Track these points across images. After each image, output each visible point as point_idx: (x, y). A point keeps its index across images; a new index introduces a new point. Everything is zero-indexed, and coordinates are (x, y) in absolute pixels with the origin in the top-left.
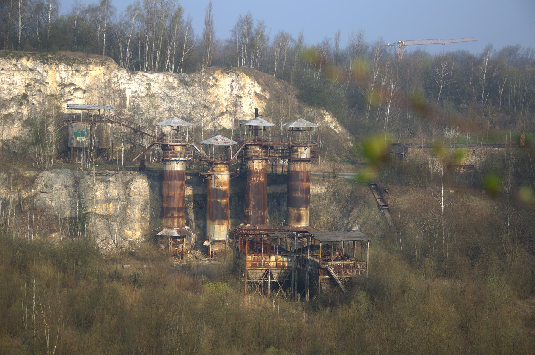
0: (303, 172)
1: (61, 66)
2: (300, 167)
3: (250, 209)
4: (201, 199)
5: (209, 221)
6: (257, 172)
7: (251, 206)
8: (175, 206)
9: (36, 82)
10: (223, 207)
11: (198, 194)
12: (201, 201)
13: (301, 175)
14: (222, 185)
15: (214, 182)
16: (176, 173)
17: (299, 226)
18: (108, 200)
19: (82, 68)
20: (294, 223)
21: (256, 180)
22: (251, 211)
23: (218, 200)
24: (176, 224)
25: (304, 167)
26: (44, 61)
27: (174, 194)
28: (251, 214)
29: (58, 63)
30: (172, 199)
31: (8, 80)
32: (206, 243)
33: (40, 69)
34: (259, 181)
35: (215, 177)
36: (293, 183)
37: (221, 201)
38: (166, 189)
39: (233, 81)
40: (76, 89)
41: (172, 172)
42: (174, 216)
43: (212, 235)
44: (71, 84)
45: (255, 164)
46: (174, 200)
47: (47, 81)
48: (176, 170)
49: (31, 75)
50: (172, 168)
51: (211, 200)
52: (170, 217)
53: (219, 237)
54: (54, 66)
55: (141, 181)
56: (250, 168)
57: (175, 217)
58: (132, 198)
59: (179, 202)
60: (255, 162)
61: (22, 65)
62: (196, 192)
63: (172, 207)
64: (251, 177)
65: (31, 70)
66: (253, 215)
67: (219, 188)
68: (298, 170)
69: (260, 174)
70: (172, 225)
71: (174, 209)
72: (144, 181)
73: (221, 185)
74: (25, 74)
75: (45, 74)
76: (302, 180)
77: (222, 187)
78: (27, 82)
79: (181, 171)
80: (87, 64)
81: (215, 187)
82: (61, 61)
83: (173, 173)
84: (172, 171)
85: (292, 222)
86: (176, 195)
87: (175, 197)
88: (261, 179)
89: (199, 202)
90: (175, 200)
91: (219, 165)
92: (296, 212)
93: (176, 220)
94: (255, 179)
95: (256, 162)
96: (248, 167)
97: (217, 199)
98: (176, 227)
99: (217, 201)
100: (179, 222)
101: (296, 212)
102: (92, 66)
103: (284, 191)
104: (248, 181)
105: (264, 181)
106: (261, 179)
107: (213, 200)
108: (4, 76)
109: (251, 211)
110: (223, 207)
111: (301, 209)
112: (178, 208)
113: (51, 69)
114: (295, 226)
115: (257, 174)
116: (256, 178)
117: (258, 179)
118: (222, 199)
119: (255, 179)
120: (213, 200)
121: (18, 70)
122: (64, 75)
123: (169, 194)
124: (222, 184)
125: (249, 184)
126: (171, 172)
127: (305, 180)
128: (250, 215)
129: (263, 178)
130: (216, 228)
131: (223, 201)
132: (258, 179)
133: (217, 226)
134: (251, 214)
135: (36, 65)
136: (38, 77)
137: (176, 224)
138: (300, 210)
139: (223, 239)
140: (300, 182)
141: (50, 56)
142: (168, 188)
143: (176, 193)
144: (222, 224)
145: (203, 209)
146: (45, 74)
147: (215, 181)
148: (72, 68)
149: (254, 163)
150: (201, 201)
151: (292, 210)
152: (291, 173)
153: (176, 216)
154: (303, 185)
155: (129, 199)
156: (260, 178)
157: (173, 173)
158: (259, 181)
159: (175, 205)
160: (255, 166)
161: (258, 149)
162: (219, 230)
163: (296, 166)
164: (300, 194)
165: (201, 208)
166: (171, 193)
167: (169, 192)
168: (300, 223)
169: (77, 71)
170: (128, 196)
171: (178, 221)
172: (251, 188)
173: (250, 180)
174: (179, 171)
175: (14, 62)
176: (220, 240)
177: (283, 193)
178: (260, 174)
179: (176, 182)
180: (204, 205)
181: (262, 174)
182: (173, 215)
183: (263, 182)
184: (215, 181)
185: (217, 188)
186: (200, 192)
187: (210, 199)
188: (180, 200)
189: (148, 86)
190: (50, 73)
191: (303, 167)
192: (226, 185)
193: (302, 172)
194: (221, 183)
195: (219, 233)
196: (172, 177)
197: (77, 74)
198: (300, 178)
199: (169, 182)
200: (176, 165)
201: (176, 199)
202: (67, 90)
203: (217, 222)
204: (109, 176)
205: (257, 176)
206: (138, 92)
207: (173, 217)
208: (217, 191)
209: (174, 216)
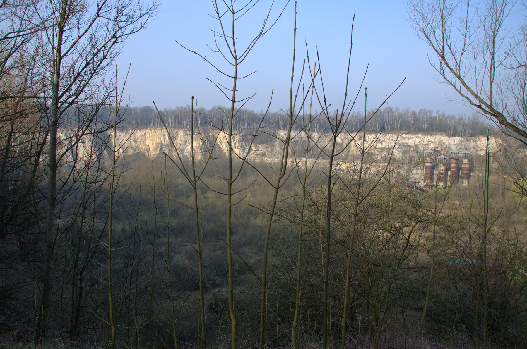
1: (429, 136)
13: (464, 169)
18: (417, 174)
19: (435, 136)
26: (424, 135)
33: (423, 137)
40: (432, 143)
44: (431, 141)
65: (420, 137)
80: (436, 135)
82: (429, 134)
102: (437, 136)
122: (429, 138)
127: (465, 170)
136: (422, 139)
175: (416, 135)
190: (426, 138)
202: (430, 143)
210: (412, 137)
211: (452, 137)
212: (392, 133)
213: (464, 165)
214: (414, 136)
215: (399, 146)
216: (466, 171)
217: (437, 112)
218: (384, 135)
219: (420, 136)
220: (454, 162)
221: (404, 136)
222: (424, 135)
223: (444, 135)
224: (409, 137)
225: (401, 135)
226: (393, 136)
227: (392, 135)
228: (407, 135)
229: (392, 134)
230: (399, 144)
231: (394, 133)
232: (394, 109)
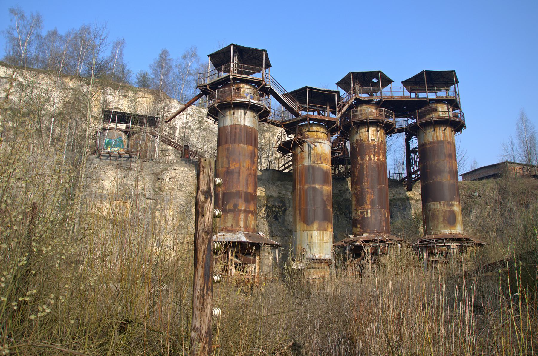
2: (445, 135)
3: (366, 206)
4: (277, 205)
5: (299, 226)
6: (374, 146)
7: (368, 203)
8: (241, 189)
10: (325, 198)
11: (272, 196)
12: (275, 208)
14: (322, 160)
15: (307, 154)
16: (243, 130)
17: (454, 232)
20: (445, 227)
21: (374, 158)
22: (369, 211)
23: (317, 186)
24: (242, 224)
25: (450, 135)
27: (240, 167)
28: (369, 215)
30: (236, 176)
32: (296, 266)
34: (379, 159)
35: (309, 146)
36: (434, 162)
37: (322, 188)
38: (225, 159)
41: (236, 129)
42: (239, 208)
43: (308, 249)
45: (369, 133)
46: (239, 179)
48: (242, 124)
50: (235, 121)
51: (303, 188)
52: (230, 211)
53: (320, 253)
55: (182, 169)
56: (361, 140)
57: (240, 211)
58: (165, 193)
59: (247, 184)
60: (369, 131)
62: (269, 194)
63: (234, 190)
64: (366, 155)
66: (373, 217)
68: (442, 139)
70: (234, 225)
71: (239, 194)
72: (187, 169)
73: (320, 159)
77: (322, 163)
79: (251, 128)
81: (311, 163)
83: (238, 130)
84: (235, 125)
85: (441, 225)
86: (242, 169)
87: (241, 174)
89: (274, 209)
90: (241, 178)
92: (446, 208)
93: (242, 216)
94: (372, 156)
95: (372, 130)
96: (357, 140)
97: (314, 183)
98: (243, 229)
99: (314, 188)
100: (249, 221)
101: (446, 208)
103: (395, 197)
104: (360, 162)
106: (380, 158)
107: (306, 186)
109: (369, 211)
110: (325, 198)
111: (453, 202)
112: (247, 193)
114: (447, 232)
115: (375, 148)
116: (374, 155)
117: (376, 157)
118: (323, 185)
119: (372, 156)
120: (306, 186)
123: (230, 167)
124: (322, 158)
125: (362, 166)
126: (234, 127)
128: (368, 217)
130: (314, 236)
131: (325, 187)
133: (315, 233)
134: (369, 215)
137: (242, 224)
138: (452, 205)
139: (328, 256)
142: (227, 158)
143: (242, 165)
144: (326, 230)
145: (280, 220)
147: (309, 154)
148: (119, 93)
149: (368, 131)
150: (275, 208)
151: (439, 205)
152: (429, 146)
153: (243, 208)
154: (452, 165)
155: (160, 194)
156: (379, 156)
157: (238, 130)
158: (379, 159)
159: (241, 188)
160: (370, 136)
161: (374, 111)
162: (320, 240)
163: (438, 134)
164: (449, 178)
165: (276, 218)
166: (233, 167)
167: (229, 163)
168: (455, 227)
169: (125, 96)
170: (158, 191)
171: (246, 219)
172: (365, 172)
173: (363, 159)
174: (247, 126)
176: (322, 258)
177: (394, 199)
178: (379, 150)
179: (242, 145)
180: (281, 214)
182: (235, 206)
184: (309, 154)
185: (313, 165)
186: (275, 194)
187: (300, 185)
188: (250, 180)
191: (448, 135)
193: (448, 143)
194: (320, 157)
195: (321, 246)
196: (235, 136)
197: (124, 99)
199: (231, 146)
200: (243, 115)
201: (243, 177)
203: (315, 225)
204: (131, 161)
206: (189, 124)
207: (235, 211)
208: (312, 169)
209: (239, 208)
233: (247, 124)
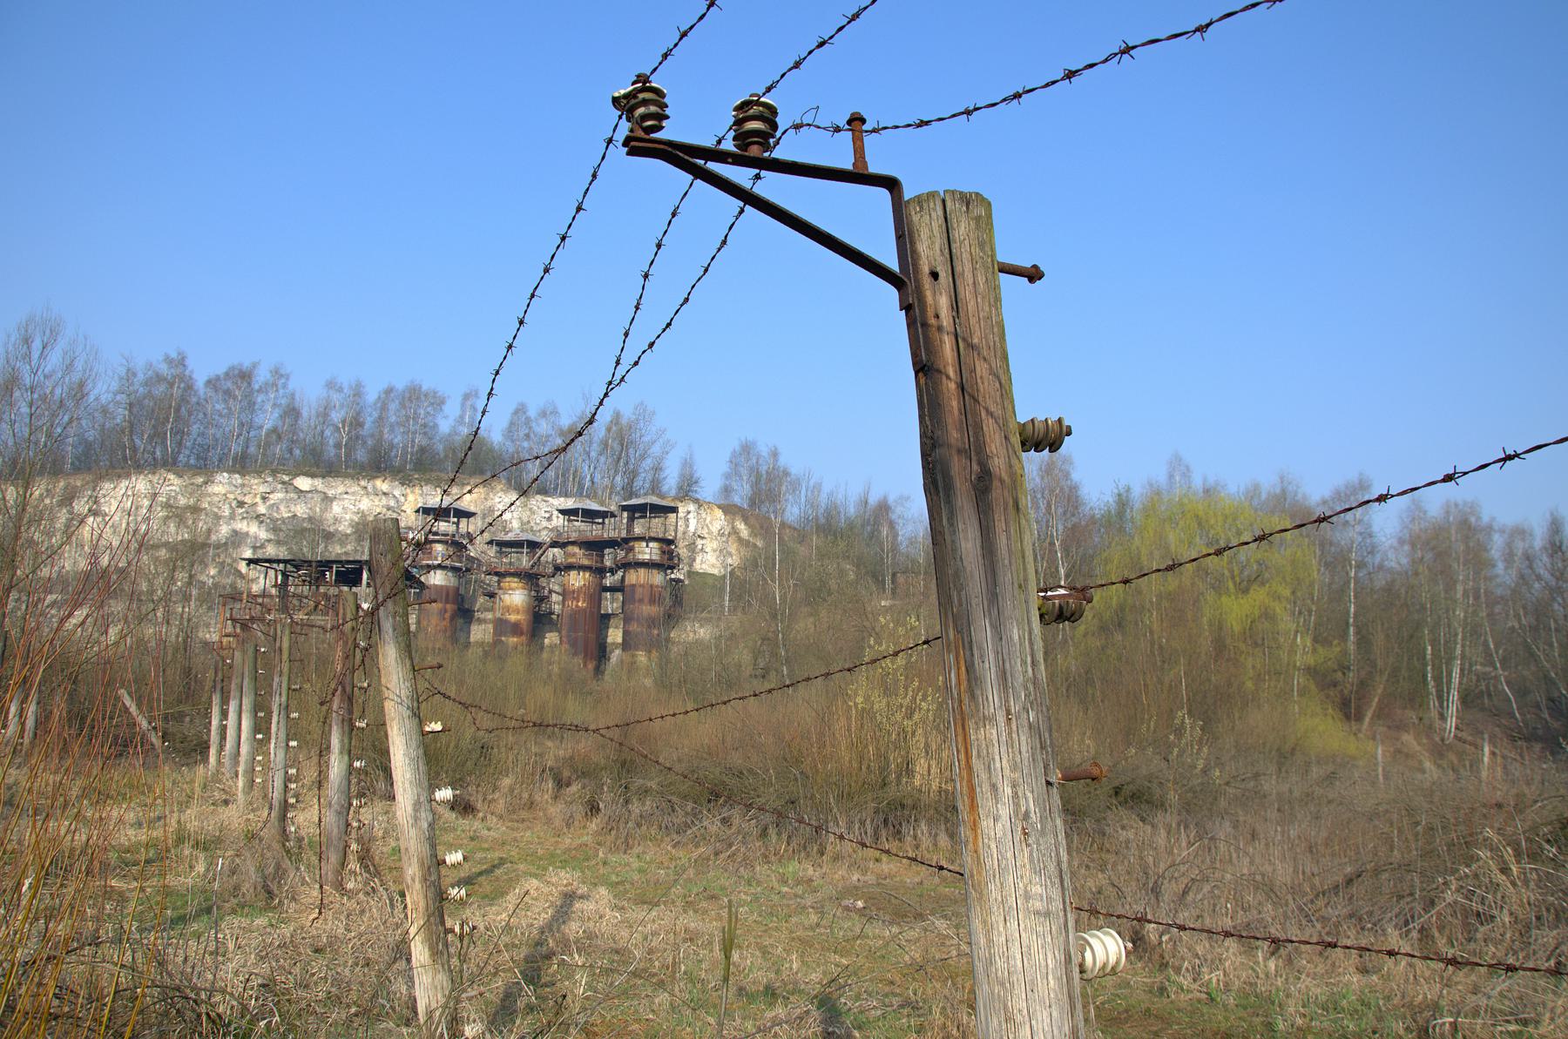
0: (642, 586)
2: (638, 577)
6: (574, 592)
9: (388, 509)
13: (639, 590)
26: (406, 481)
29: (423, 484)
31: (352, 507)
33: (397, 493)
39: (689, 512)
47: (403, 508)
49: (384, 501)
54: (417, 490)
61: (374, 487)
65: (385, 494)
67: (504, 617)
69: (578, 596)
74: (376, 500)
75: (402, 499)
76: (641, 601)
78: (378, 511)
79: (442, 586)
82: (428, 482)
88: (580, 604)
91: (508, 579)
95: (573, 573)
105: (587, 607)
106: (580, 604)
108: (346, 501)
113: (412, 492)
117: (574, 603)
121: (368, 494)
127: (646, 600)
129: (584, 601)
132: (574, 603)
135: (393, 488)
136: (392, 503)
140: (637, 604)
141: (416, 476)
146: (402, 499)
158: (577, 606)
175: (363, 483)
181: (582, 595)
183: (584, 610)
189: (547, 515)
190: (411, 498)
192: (518, 613)
194: (508, 609)
198: (637, 596)
205: (574, 598)
206: (532, 524)
210: (341, 489)
211: (539, 497)
212: (239, 473)
213: (642, 571)
214: (356, 488)
215: (275, 530)
216: (652, 601)
217: (466, 397)
218: (200, 480)
219: (382, 485)
220: (586, 562)
221: (303, 483)
222: (403, 484)
223: (499, 487)
224: (331, 493)
225: (286, 478)
226: (243, 485)
227: (237, 479)
228: (319, 483)
229: (243, 475)
230: (274, 520)
231: (249, 473)
232: (262, 376)
233: (437, 583)
